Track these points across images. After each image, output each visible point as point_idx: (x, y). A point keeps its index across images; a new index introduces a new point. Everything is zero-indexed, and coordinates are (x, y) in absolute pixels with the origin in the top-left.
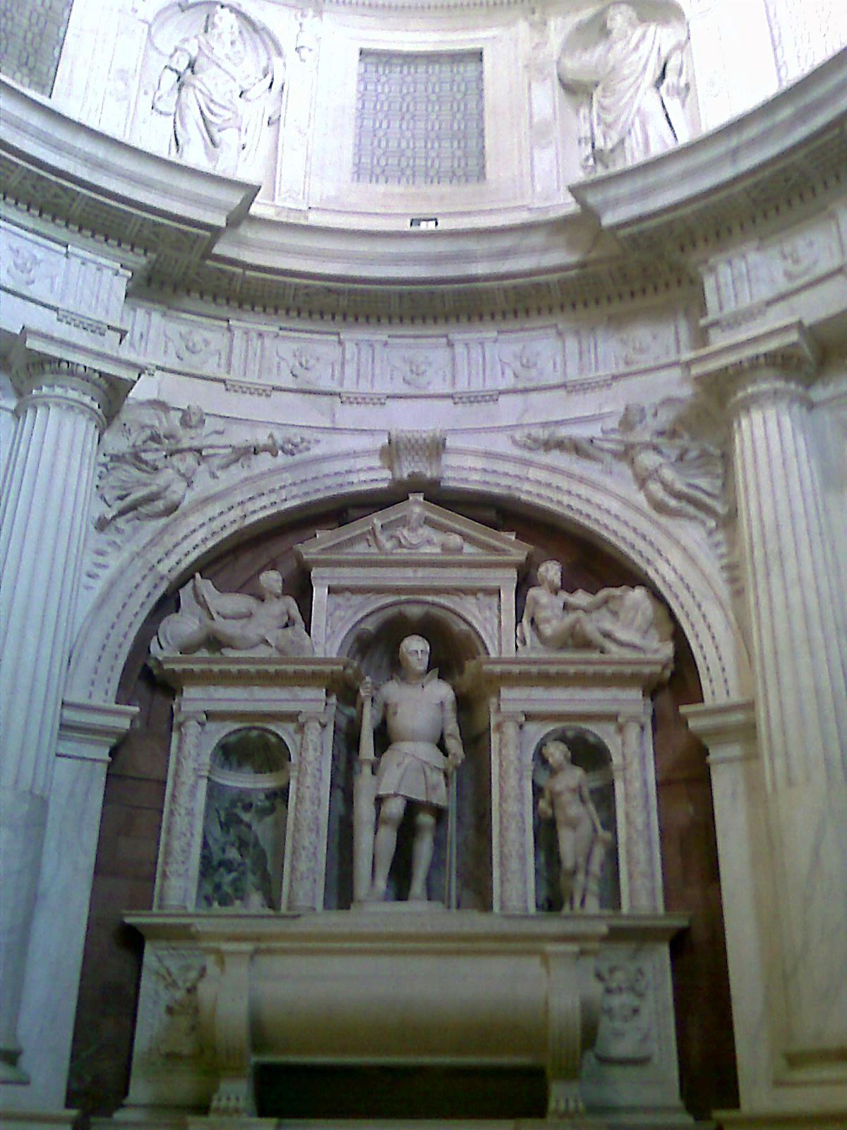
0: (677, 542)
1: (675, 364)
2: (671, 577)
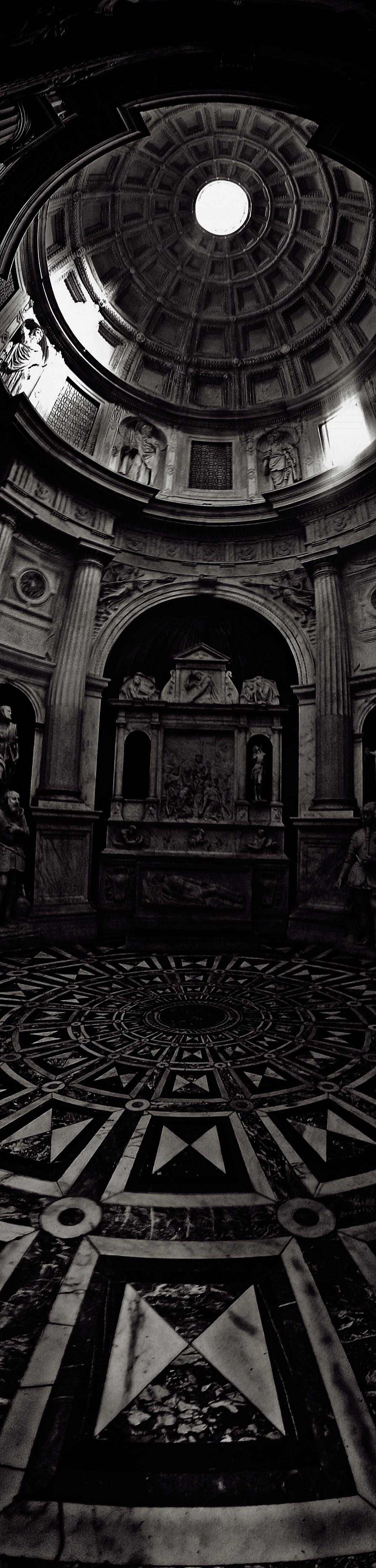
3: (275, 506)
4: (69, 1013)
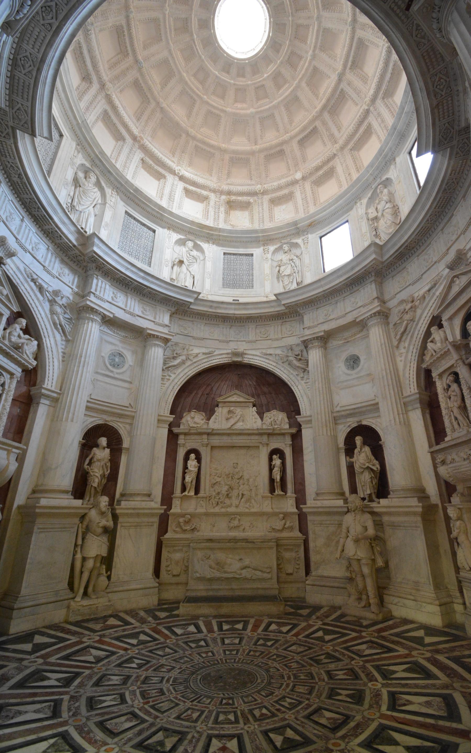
0: (54, 337)
1: (72, 289)
2: (49, 345)
3: (283, 302)
4: (129, 677)
